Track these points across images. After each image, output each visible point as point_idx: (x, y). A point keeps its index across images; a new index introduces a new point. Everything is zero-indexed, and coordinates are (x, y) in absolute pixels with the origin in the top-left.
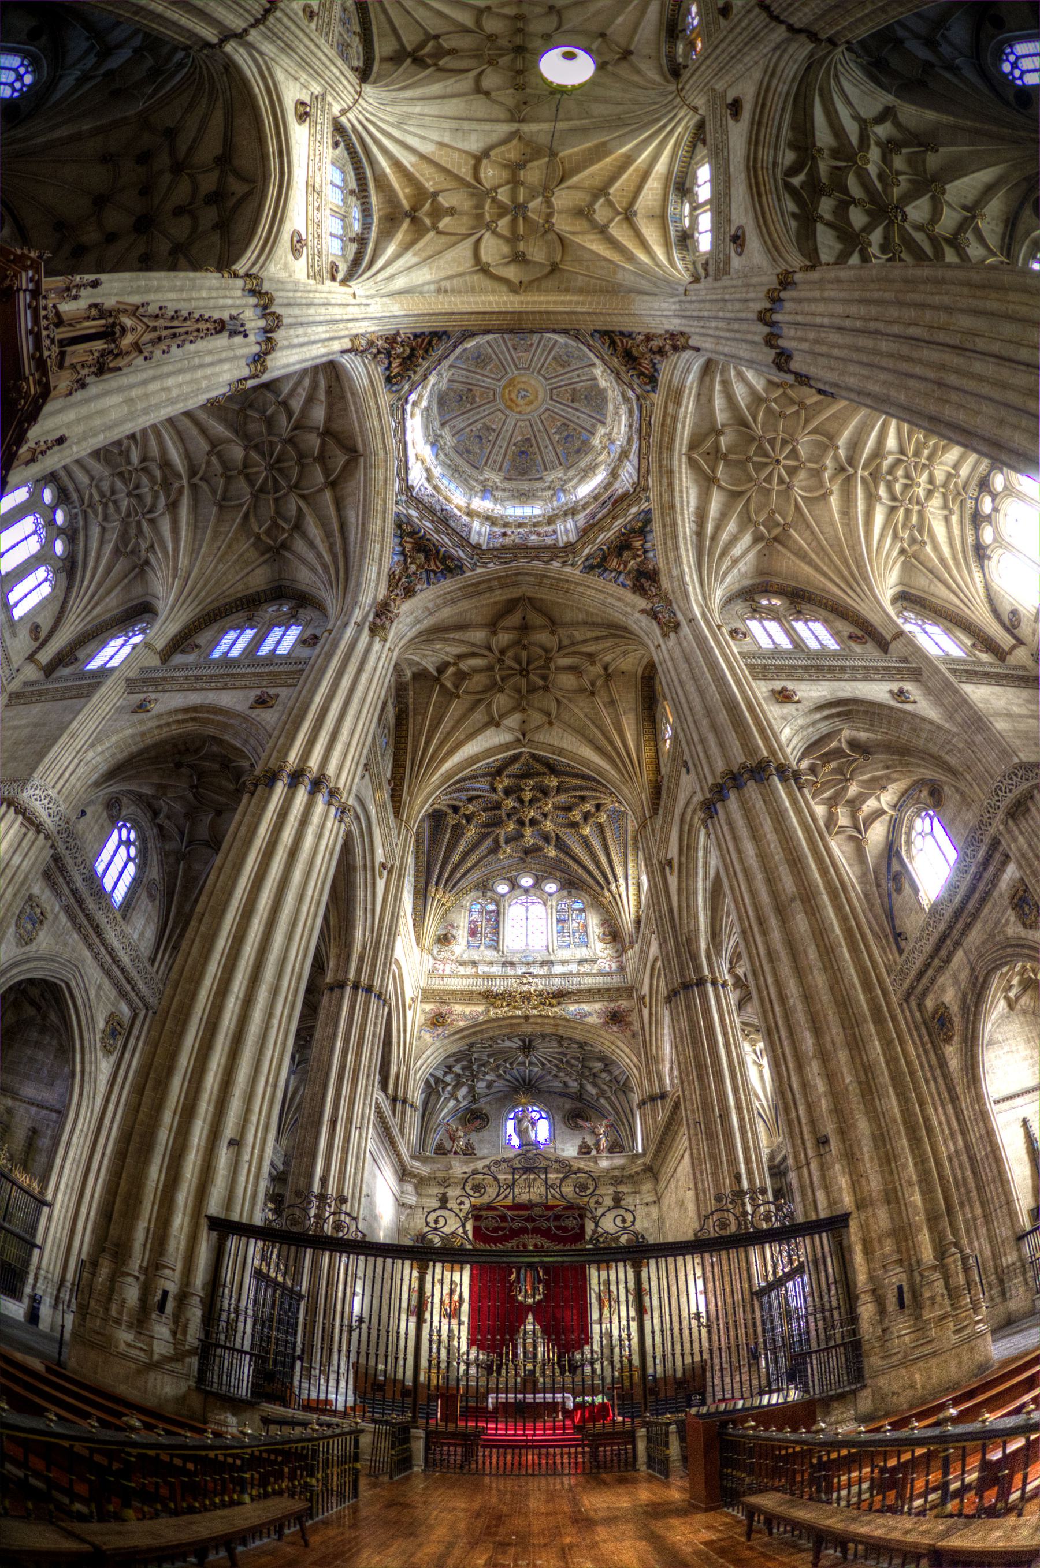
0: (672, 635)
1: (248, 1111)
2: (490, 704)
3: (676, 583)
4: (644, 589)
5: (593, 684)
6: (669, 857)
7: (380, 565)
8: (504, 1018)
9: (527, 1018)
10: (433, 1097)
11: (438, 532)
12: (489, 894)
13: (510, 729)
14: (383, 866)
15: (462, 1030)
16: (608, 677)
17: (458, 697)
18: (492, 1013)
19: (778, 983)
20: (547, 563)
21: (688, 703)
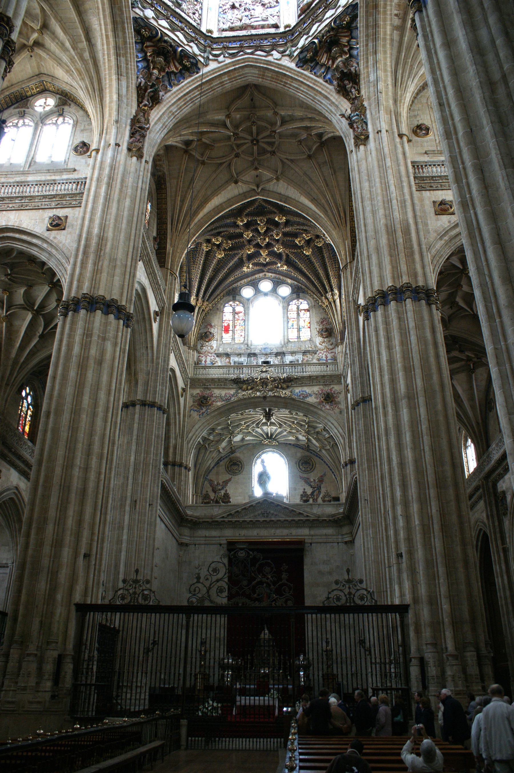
0: (362, 147)
2: (229, 165)
3: (372, 89)
4: (346, 90)
5: (310, 150)
6: (359, 303)
7: (128, 78)
8: (249, 398)
9: (265, 397)
10: (203, 451)
11: (173, 30)
12: (237, 297)
13: (245, 182)
14: (156, 313)
15: (219, 408)
16: (323, 144)
17: (203, 163)
18: (240, 395)
19: (388, 449)
20: (269, 53)
21: (364, 219)
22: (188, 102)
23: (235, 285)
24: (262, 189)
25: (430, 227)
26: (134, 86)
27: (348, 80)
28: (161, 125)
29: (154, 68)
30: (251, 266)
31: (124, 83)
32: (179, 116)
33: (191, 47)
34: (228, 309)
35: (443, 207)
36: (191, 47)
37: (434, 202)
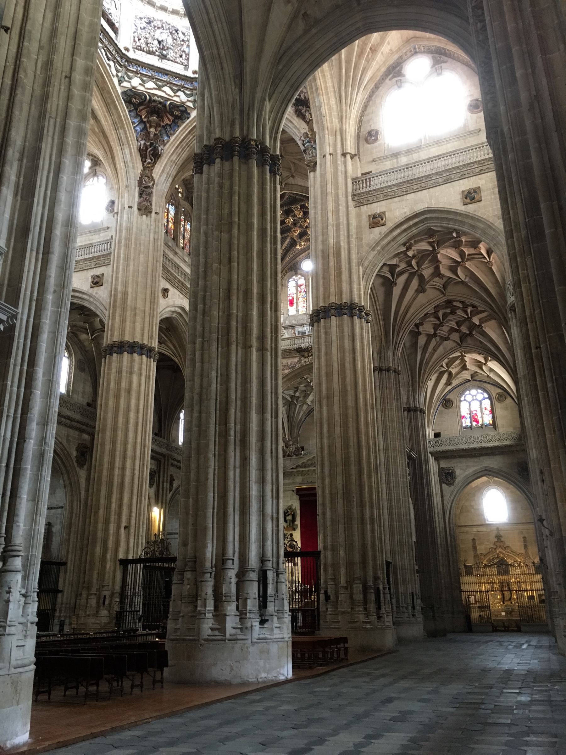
1: (131, 512)
4: (302, 114)
10: (293, 406)
11: (159, 88)
12: (299, 271)
15: (287, 375)
22: (185, 147)
23: (294, 262)
24: (286, 184)
25: (364, 242)
26: (136, 150)
27: (301, 105)
28: (165, 175)
29: (150, 128)
30: (303, 243)
31: (127, 151)
32: (180, 163)
33: (179, 96)
34: (292, 284)
35: (375, 220)
36: (179, 96)
37: (369, 216)
